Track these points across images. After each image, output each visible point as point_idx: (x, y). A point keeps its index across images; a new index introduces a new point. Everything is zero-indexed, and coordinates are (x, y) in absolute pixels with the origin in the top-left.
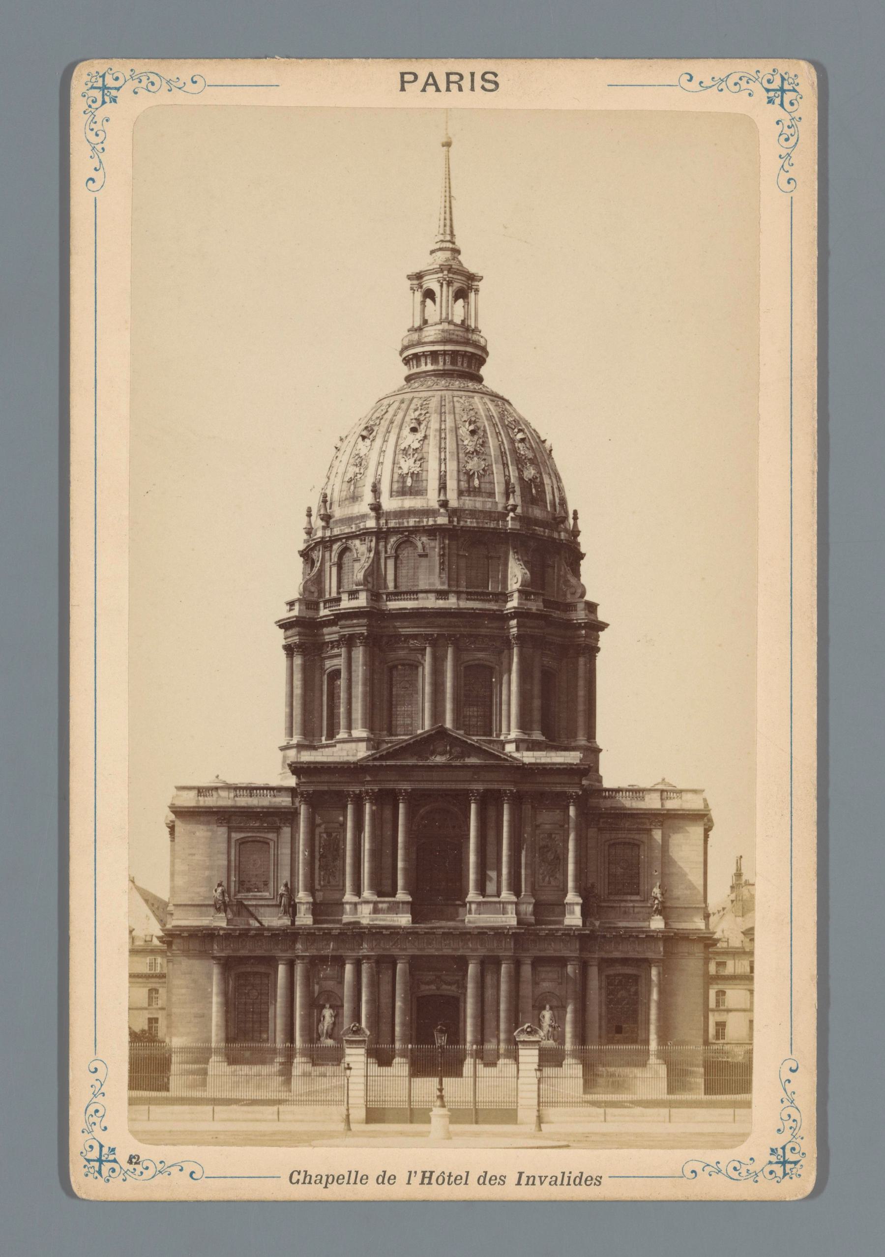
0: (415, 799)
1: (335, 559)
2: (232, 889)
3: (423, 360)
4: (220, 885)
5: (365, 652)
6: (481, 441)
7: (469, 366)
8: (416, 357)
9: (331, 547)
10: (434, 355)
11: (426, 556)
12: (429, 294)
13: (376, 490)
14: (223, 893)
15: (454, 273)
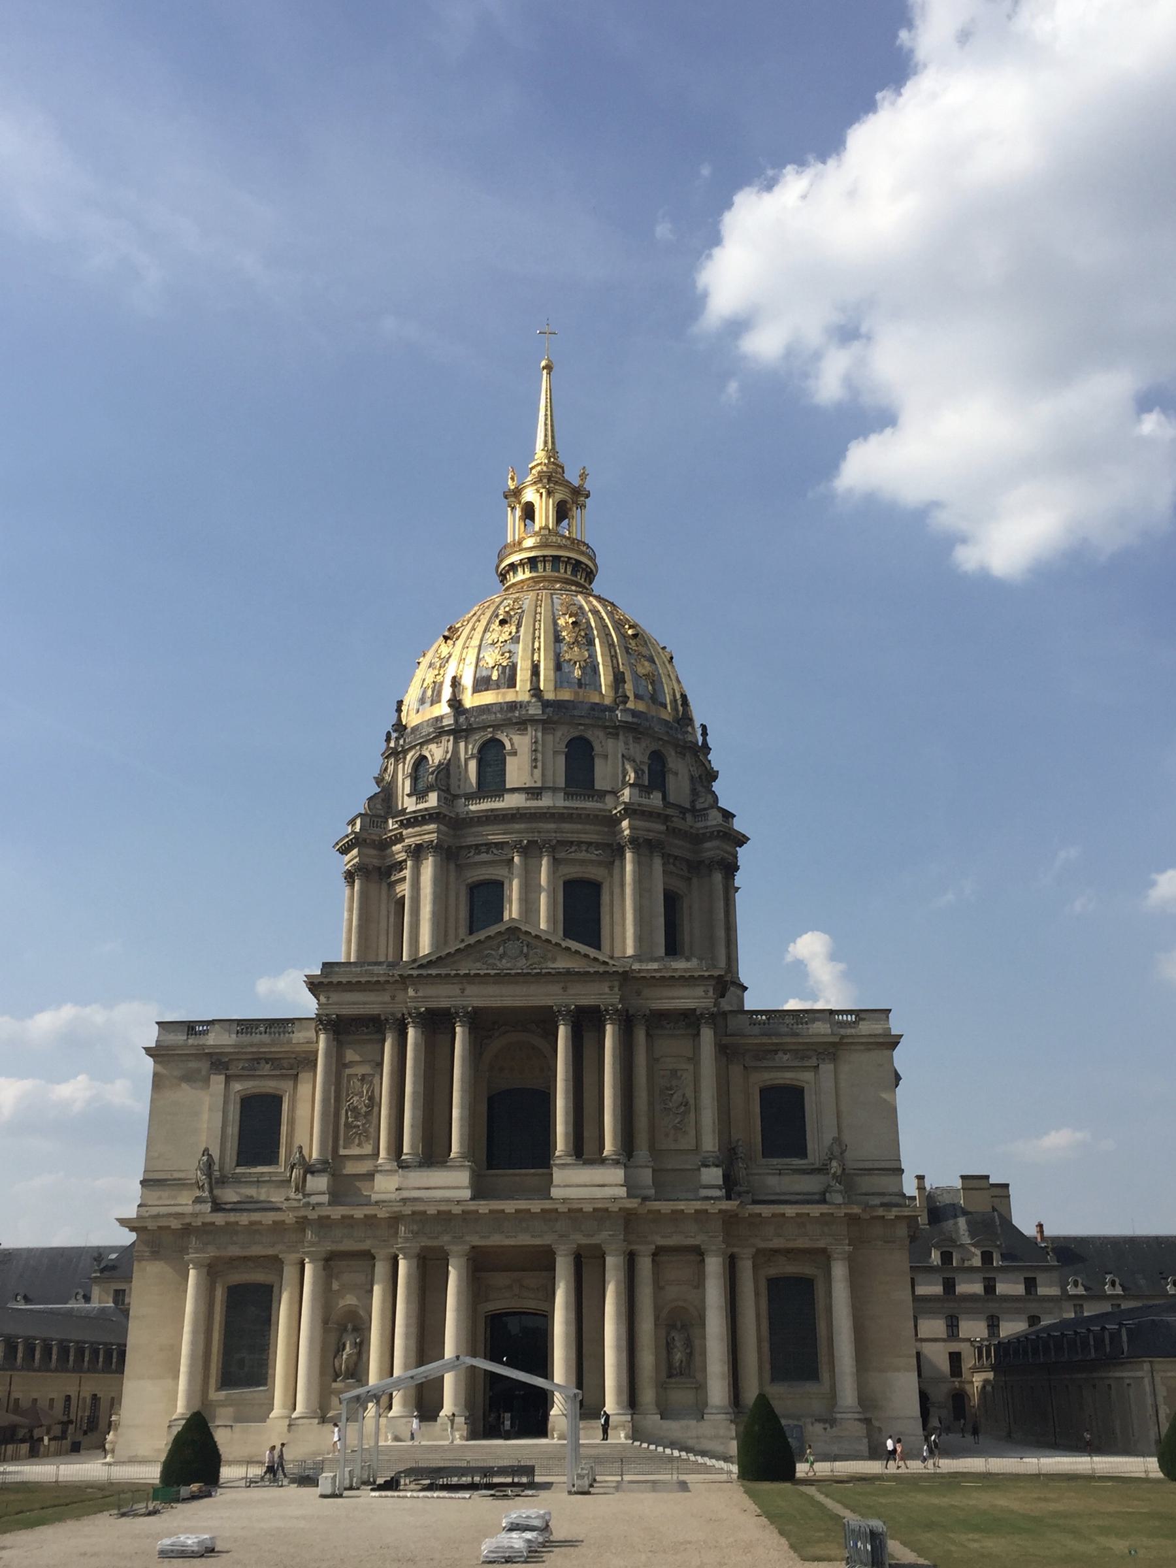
0: (483, 1024)
1: (408, 768)
2: (228, 1160)
3: (520, 570)
4: (206, 1152)
5: (435, 866)
6: (583, 633)
7: (574, 573)
8: (513, 567)
9: (405, 758)
10: (532, 562)
11: (514, 753)
12: (529, 512)
13: (455, 683)
14: (210, 1164)
15: (556, 483)
